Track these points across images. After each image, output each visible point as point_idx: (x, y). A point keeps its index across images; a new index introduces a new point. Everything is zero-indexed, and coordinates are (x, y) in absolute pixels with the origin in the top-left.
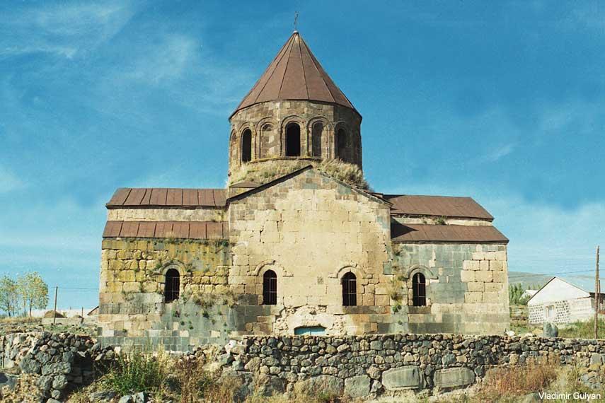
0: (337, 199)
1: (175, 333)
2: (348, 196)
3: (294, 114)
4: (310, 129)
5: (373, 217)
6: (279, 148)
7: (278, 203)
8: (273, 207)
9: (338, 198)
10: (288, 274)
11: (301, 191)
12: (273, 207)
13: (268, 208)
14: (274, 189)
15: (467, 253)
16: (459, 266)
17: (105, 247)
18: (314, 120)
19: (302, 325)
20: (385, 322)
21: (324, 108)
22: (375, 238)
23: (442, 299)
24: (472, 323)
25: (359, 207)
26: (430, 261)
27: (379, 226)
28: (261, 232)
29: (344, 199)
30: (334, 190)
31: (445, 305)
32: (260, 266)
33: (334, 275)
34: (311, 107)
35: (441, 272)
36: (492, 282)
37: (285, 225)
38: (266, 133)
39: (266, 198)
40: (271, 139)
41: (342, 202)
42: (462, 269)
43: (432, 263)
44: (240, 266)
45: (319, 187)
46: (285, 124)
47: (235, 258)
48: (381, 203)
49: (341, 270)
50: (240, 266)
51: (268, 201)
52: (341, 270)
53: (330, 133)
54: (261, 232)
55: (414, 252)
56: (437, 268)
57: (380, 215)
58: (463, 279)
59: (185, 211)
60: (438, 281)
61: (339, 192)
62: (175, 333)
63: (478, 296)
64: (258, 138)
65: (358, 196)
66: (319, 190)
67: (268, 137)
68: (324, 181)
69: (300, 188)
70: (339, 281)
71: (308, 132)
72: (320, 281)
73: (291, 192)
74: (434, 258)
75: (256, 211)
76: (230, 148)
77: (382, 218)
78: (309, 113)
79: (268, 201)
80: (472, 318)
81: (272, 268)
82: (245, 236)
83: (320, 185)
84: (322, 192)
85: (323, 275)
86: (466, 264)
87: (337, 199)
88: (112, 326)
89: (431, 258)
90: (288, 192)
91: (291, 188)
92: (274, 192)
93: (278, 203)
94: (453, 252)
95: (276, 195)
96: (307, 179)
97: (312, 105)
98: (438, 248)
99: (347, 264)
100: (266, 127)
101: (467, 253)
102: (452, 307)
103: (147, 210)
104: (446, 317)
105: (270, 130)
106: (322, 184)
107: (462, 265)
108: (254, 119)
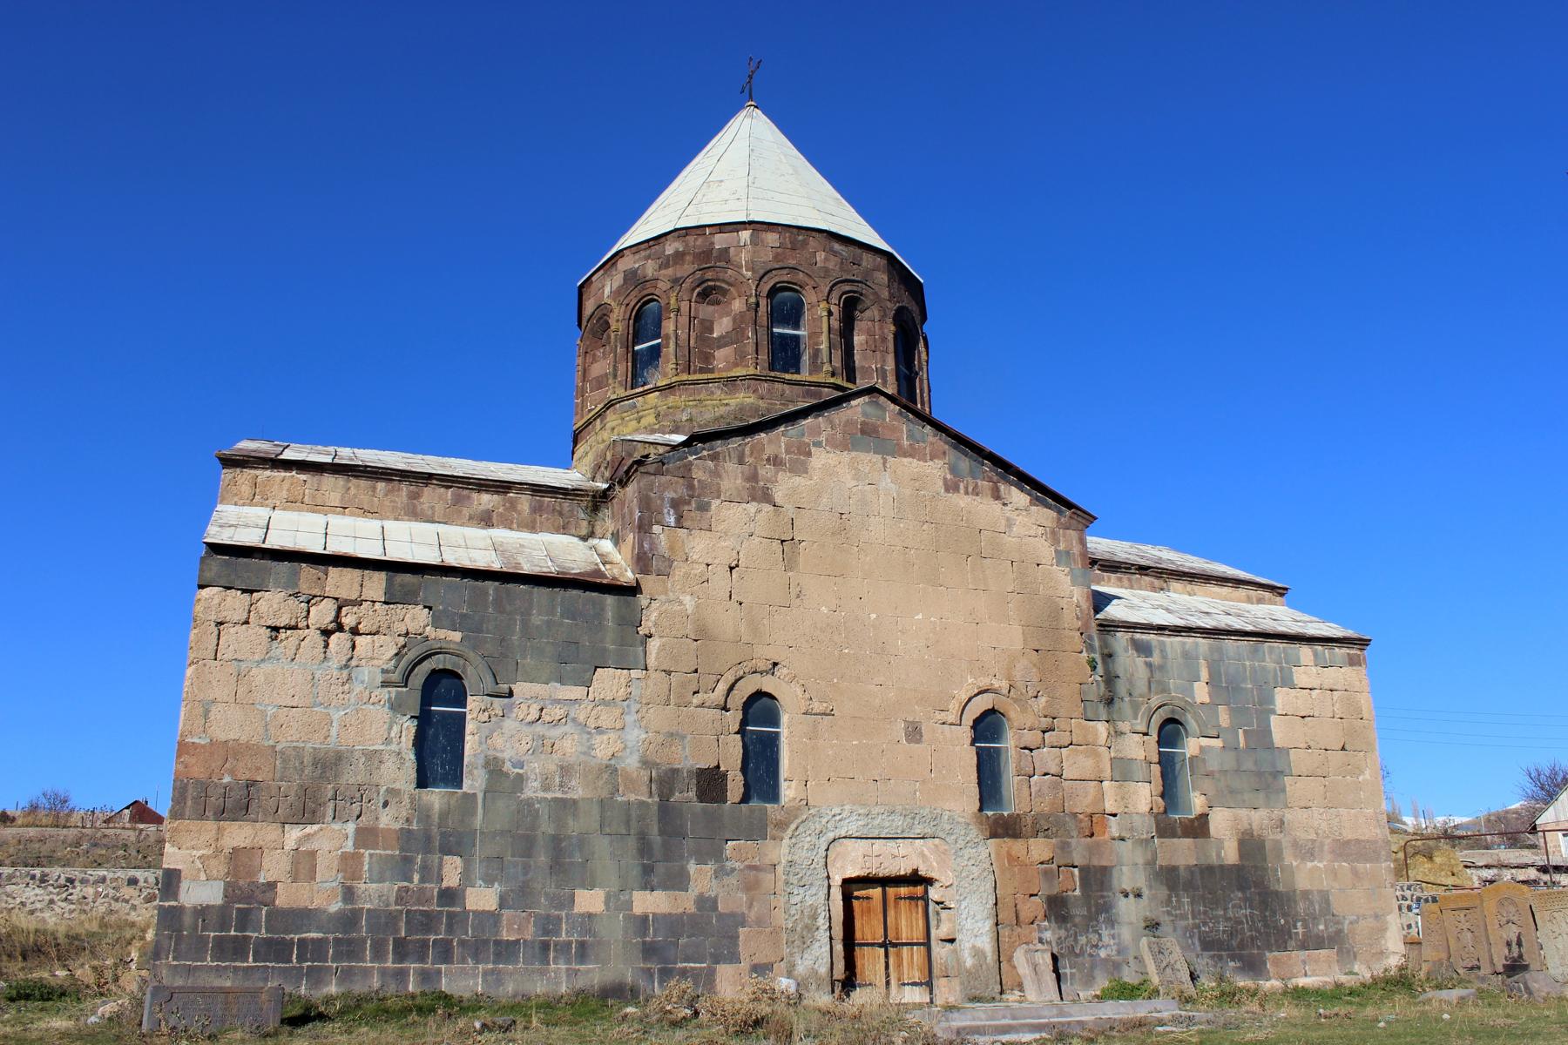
0: (947, 490)
1: (450, 896)
2: (977, 485)
3: (792, 263)
4: (834, 309)
5: (1046, 551)
6: (751, 349)
7: (785, 486)
8: (765, 497)
9: (951, 487)
10: (817, 707)
11: (846, 457)
12: (765, 497)
13: (754, 499)
14: (776, 442)
15: (1282, 669)
16: (1265, 707)
17: (209, 575)
18: (847, 288)
19: (863, 873)
20: (1095, 862)
21: (864, 264)
22: (1056, 612)
23: (1228, 796)
24: (1309, 865)
25: (1008, 519)
26: (1196, 684)
27: (1061, 575)
28: (732, 569)
29: (967, 493)
30: (939, 463)
31: (1243, 812)
32: (730, 677)
33: (952, 717)
34: (835, 253)
35: (1224, 717)
36: (1343, 749)
37: (806, 553)
38: (705, 310)
39: (745, 467)
40: (722, 327)
41: (962, 501)
42: (1273, 712)
43: (1201, 693)
44: (669, 673)
45: (901, 452)
46: (765, 288)
47: (654, 645)
48: (1060, 512)
49: (970, 700)
50: (669, 673)
51: (753, 477)
52: (970, 700)
53: (881, 328)
54: (732, 569)
55: (1156, 659)
56: (1213, 705)
57: (1062, 547)
58: (1279, 736)
59: (475, 495)
60: (1217, 743)
61: (953, 469)
62: (450, 896)
63: (1314, 785)
64: (684, 320)
65: (1002, 487)
66: (898, 460)
67: (712, 323)
68: (910, 436)
69: (844, 446)
70: (965, 733)
71: (830, 313)
72: (914, 733)
73: (821, 459)
74: (1204, 674)
75: (715, 503)
76: (580, 360)
77: (1068, 553)
78: (831, 265)
79: (753, 477)
80: (1308, 851)
81: (767, 684)
82: (687, 575)
83: (899, 445)
84: (910, 465)
85: (918, 713)
86: (1282, 698)
87: (947, 490)
88: (219, 867)
89: (1198, 680)
90: (809, 454)
91: (818, 444)
92: (769, 451)
93: (785, 486)
94: (1248, 663)
95: (775, 461)
96: (863, 423)
97: (837, 246)
98: (1211, 648)
99: (984, 682)
100: (708, 293)
101: (1282, 669)
102: (1258, 819)
103: (354, 481)
104: (1251, 845)
105: (718, 303)
106: (906, 443)
107: (1271, 700)
108: (670, 271)
